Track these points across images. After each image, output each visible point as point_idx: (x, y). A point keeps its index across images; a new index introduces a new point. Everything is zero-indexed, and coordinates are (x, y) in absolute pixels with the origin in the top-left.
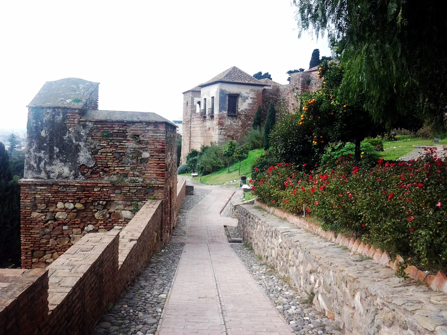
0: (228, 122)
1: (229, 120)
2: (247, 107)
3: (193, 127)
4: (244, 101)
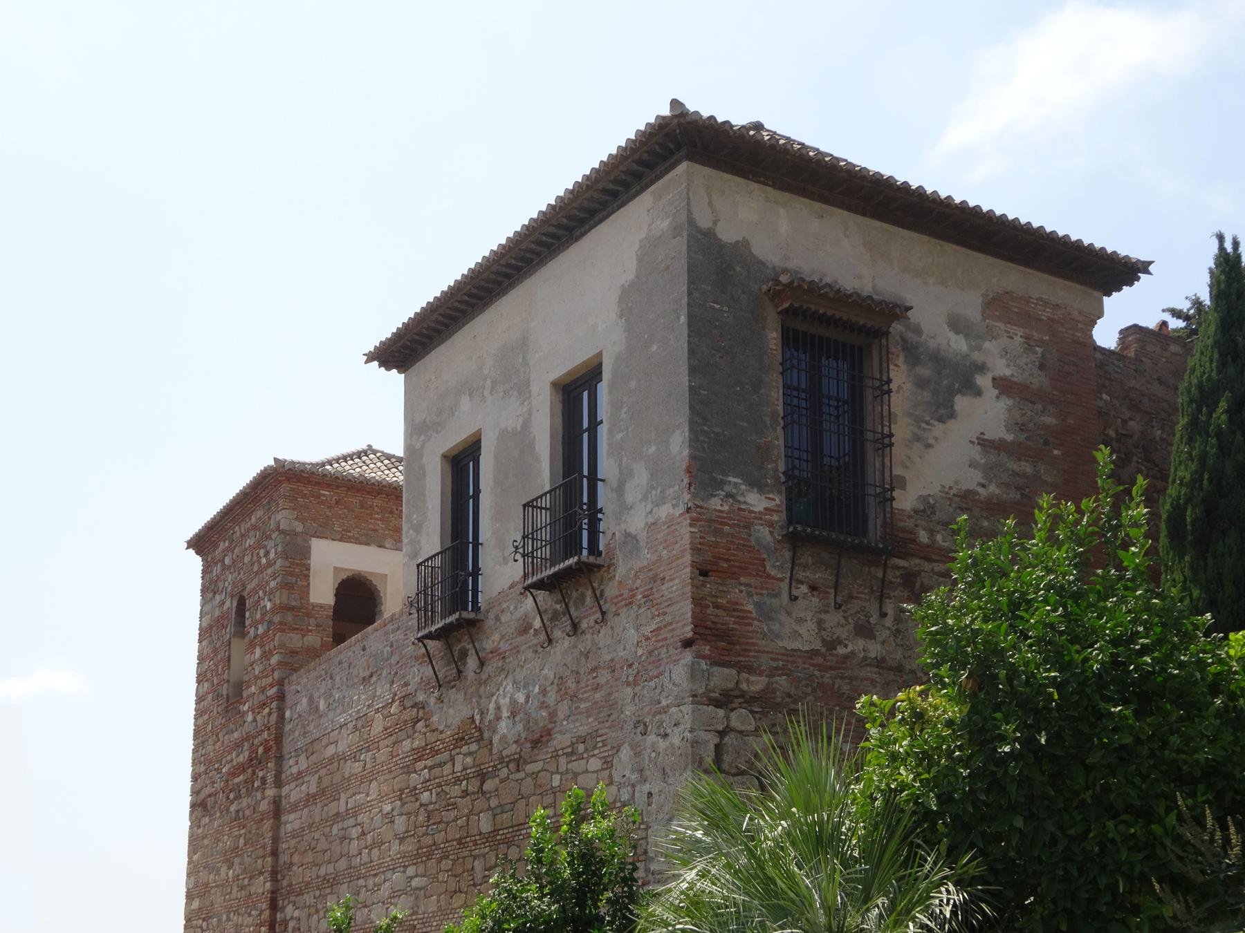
1: (809, 605)
2: (971, 480)
3: (310, 799)
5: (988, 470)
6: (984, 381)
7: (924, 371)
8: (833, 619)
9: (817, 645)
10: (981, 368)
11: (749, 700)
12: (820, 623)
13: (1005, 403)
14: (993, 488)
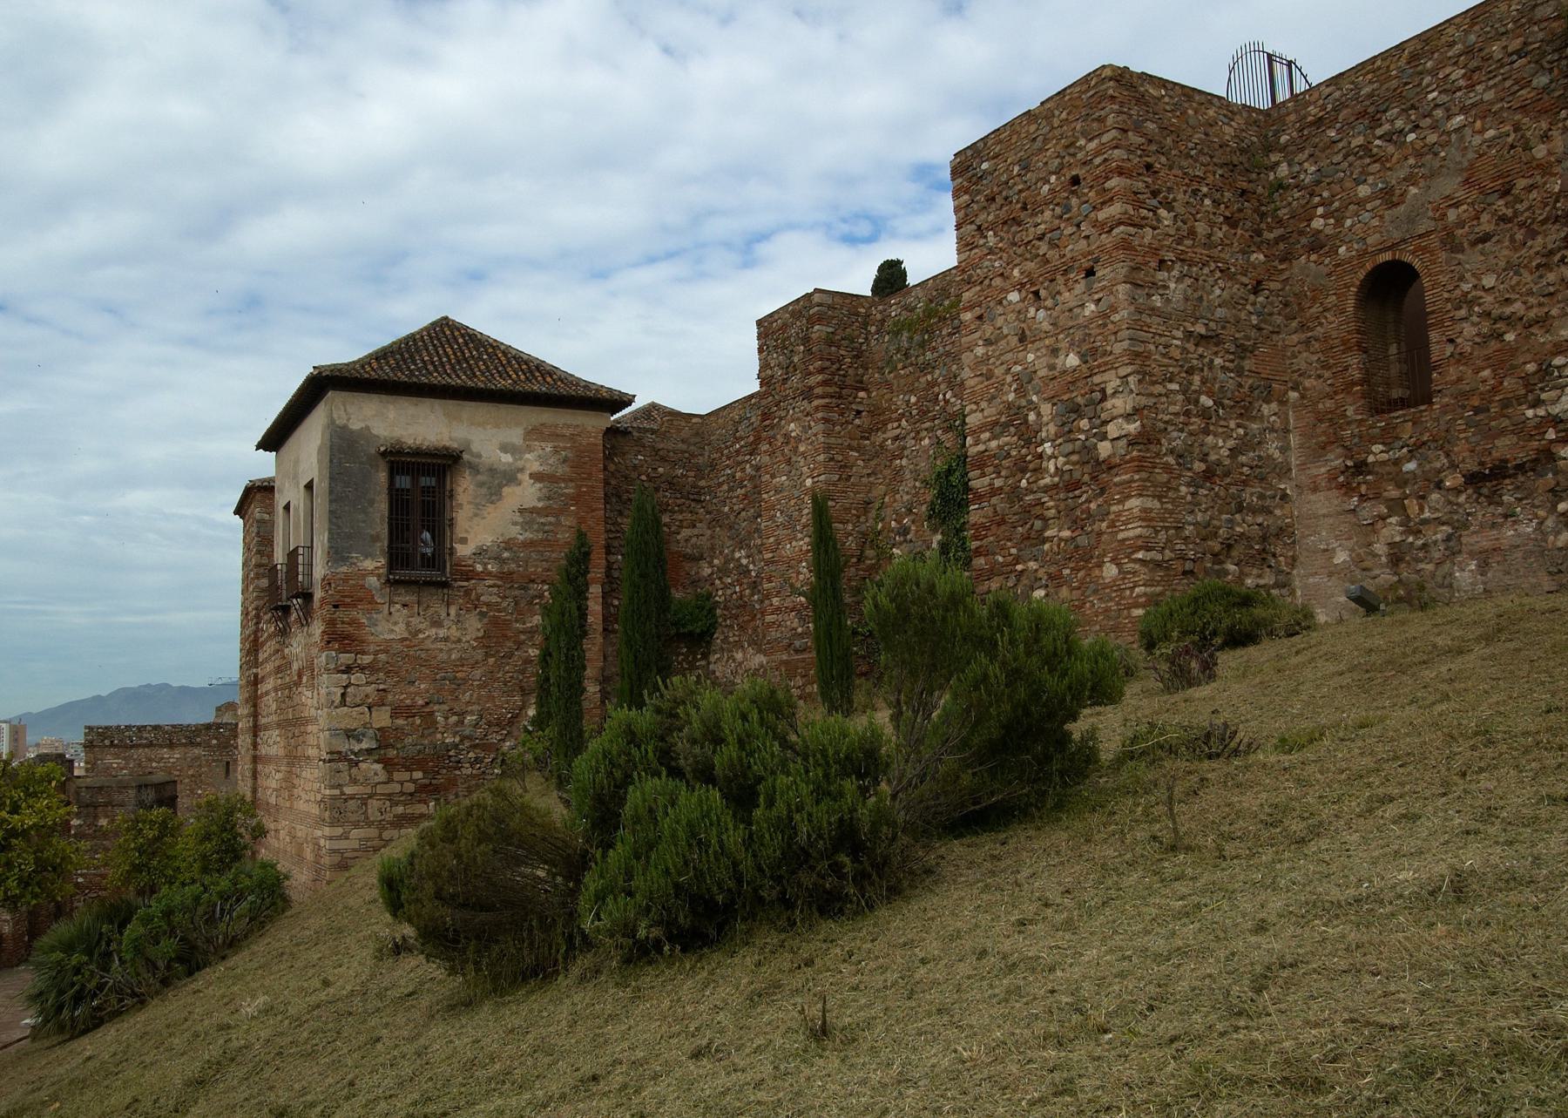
0: (390, 624)
2: (515, 532)
4: (494, 495)
5: (526, 525)
6: (525, 477)
7: (479, 477)
8: (415, 621)
9: (406, 635)
10: (521, 470)
11: (362, 669)
12: (408, 624)
13: (538, 485)
14: (528, 535)
